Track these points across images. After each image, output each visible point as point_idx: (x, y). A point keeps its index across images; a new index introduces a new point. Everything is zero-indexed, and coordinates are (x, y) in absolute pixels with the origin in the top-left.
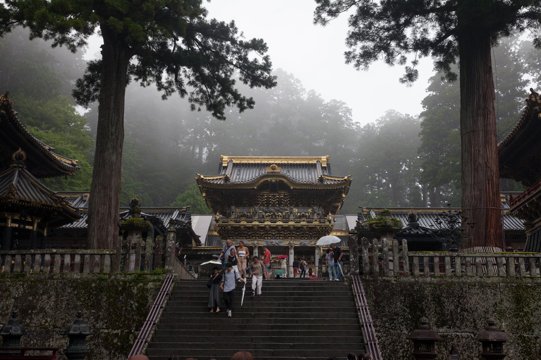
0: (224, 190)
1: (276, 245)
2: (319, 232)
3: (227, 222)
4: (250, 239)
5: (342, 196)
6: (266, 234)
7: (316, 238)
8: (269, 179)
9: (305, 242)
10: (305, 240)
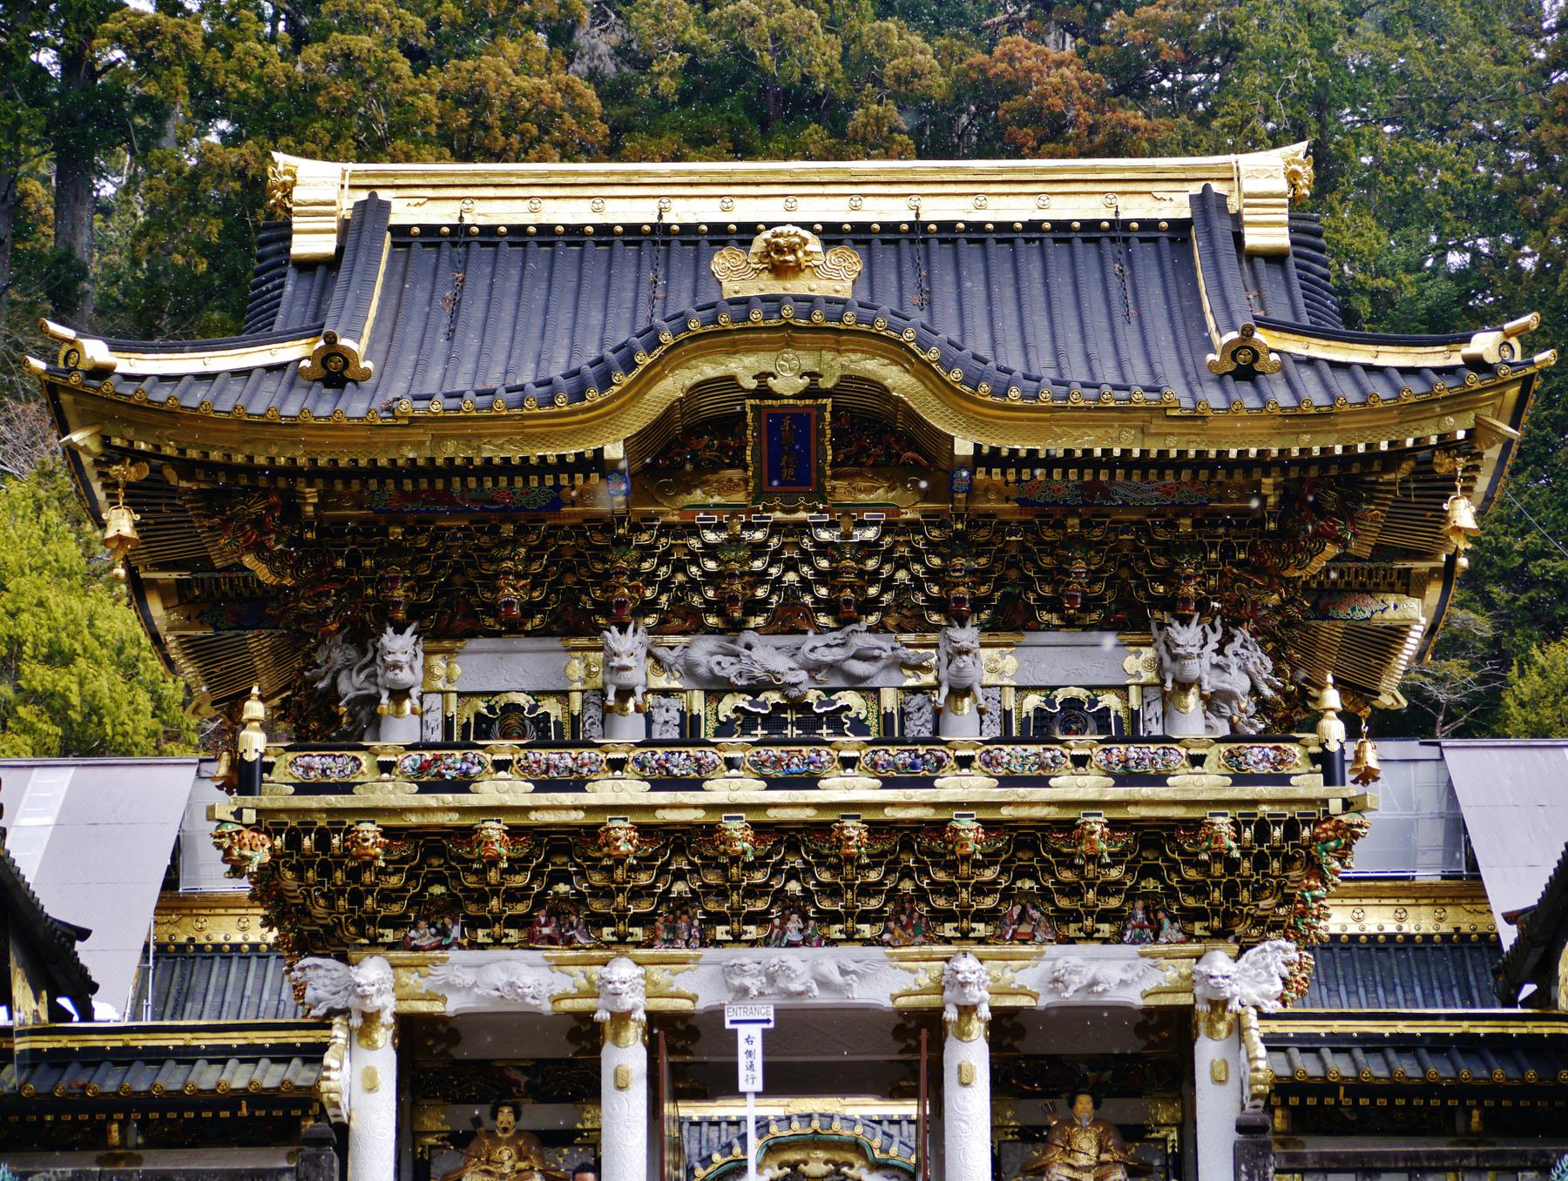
0: (313, 474)
1: (820, 998)
2: (1232, 865)
3: (347, 788)
4: (569, 942)
5: (1443, 516)
6: (722, 893)
7: (1198, 928)
8: (744, 367)
9: (1091, 971)
10: (1094, 948)
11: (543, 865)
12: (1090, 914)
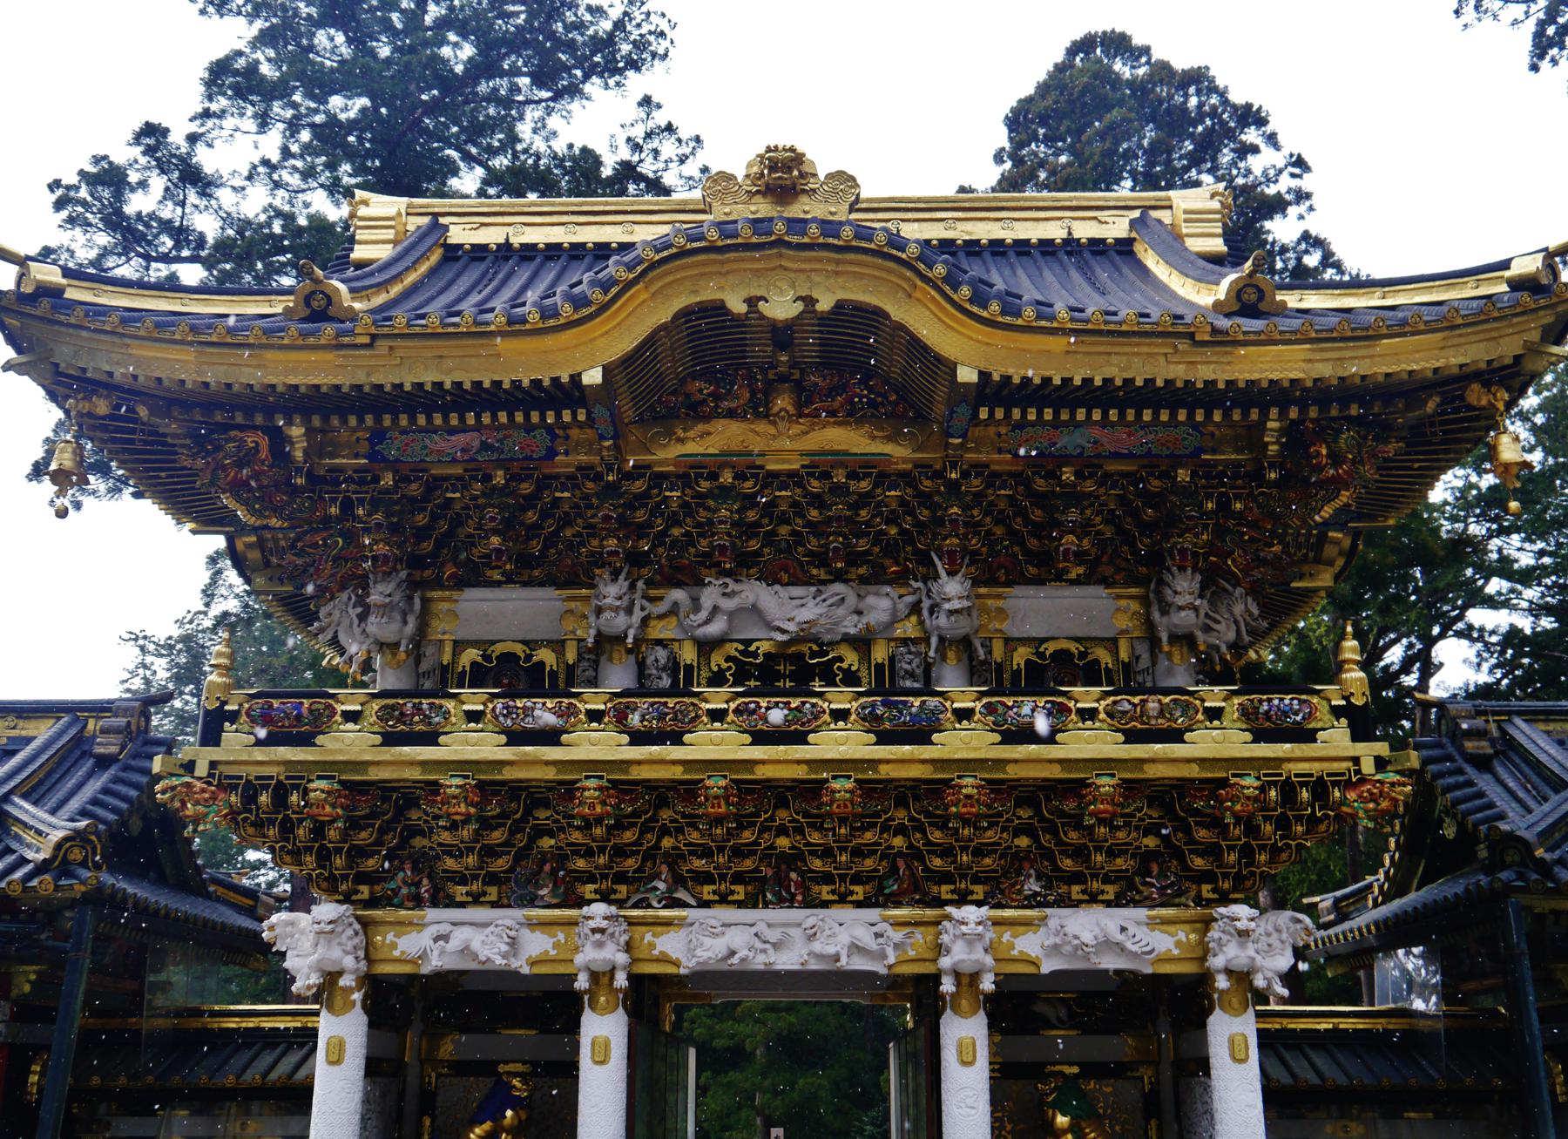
11: (524, 820)
12: (1095, 876)
